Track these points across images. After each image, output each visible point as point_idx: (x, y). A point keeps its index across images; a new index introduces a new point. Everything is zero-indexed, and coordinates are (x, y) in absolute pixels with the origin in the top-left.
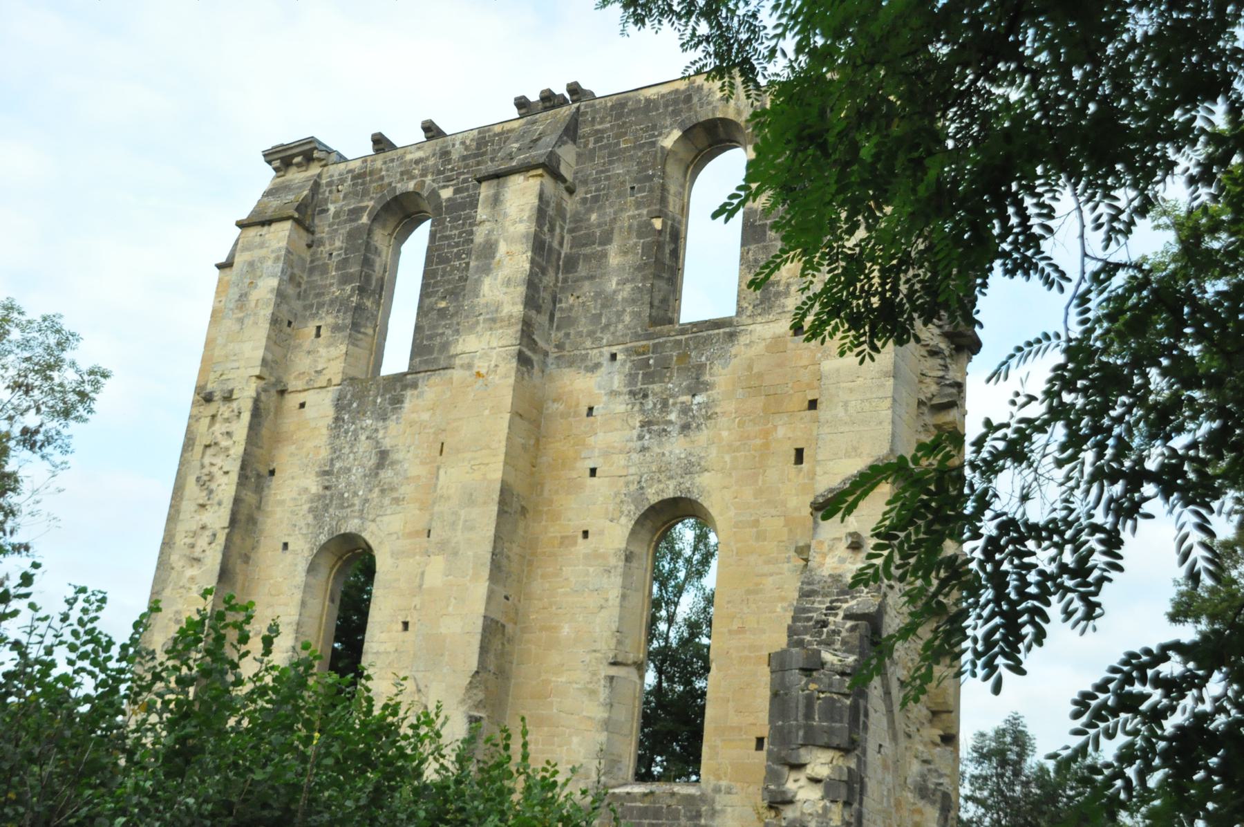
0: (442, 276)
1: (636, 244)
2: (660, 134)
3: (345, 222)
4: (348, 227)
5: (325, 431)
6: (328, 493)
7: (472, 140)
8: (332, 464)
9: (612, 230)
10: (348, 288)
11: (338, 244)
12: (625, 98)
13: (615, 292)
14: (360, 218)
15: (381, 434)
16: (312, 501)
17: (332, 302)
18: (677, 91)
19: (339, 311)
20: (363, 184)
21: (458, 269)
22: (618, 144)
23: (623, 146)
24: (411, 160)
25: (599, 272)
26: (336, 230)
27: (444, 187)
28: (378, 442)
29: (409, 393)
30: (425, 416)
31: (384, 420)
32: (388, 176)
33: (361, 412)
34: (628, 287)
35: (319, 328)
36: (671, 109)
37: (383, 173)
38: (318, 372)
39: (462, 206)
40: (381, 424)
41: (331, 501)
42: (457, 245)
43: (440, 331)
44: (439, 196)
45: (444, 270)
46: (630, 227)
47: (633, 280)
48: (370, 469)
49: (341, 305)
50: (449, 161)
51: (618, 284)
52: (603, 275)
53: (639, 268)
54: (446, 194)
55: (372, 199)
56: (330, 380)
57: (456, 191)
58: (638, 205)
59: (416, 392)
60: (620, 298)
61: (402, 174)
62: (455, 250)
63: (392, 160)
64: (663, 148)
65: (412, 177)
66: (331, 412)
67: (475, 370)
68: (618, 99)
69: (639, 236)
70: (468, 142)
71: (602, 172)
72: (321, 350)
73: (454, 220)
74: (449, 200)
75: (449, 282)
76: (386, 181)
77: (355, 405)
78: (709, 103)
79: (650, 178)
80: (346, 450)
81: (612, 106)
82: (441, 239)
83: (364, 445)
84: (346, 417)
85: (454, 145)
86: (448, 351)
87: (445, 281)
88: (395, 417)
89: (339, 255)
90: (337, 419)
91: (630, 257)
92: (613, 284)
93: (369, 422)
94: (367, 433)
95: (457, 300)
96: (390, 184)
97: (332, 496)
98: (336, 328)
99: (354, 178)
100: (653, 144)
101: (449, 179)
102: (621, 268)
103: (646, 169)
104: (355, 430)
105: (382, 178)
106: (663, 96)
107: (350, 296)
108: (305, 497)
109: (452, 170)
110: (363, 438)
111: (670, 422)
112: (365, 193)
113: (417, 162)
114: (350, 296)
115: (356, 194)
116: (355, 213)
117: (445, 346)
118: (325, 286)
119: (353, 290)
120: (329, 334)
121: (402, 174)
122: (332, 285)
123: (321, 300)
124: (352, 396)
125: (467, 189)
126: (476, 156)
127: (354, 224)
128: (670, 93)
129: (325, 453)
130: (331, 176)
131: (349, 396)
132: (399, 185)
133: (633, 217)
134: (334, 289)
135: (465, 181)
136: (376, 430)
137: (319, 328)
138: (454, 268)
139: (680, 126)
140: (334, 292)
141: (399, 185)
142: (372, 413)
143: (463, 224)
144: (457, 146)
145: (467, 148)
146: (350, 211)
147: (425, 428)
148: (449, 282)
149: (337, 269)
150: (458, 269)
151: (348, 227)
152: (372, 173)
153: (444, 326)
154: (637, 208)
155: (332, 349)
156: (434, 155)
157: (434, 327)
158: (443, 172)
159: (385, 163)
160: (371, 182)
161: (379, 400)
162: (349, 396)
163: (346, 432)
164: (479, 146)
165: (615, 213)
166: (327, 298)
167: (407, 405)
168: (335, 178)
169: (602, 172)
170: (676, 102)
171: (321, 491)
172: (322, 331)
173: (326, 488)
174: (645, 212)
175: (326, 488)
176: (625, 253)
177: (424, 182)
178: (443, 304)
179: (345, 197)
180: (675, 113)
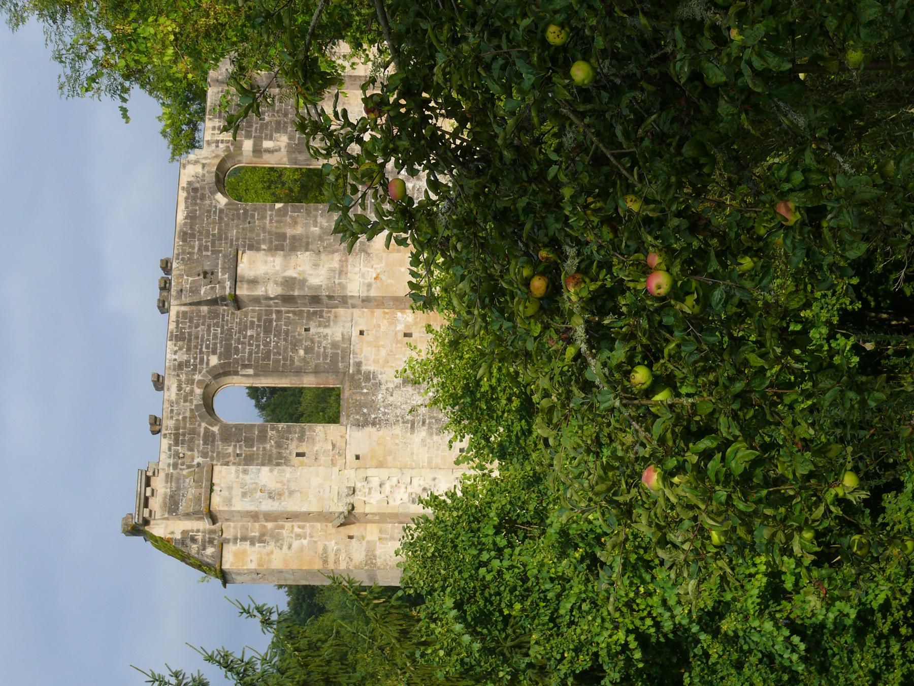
0: (280, 354)
1: (291, 217)
2: (215, 207)
3: (213, 446)
4: (218, 443)
5: (381, 433)
6: (427, 421)
7: (175, 345)
8: (407, 422)
9: (276, 233)
10: (270, 433)
11: (230, 450)
12: (180, 233)
13: (321, 228)
14: (213, 434)
15: (391, 385)
16: (431, 434)
17: (279, 445)
18: (187, 198)
19: (287, 439)
20: (184, 435)
21: (277, 343)
22: (214, 235)
23: (216, 232)
24: (177, 394)
25: (304, 240)
26: (218, 453)
27: (208, 364)
28: (396, 387)
29: (364, 368)
30: (383, 352)
31: (380, 384)
32: (184, 413)
33: (372, 406)
34: (319, 219)
35: (298, 455)
36: (198, 201)
37: (180, 417)
38: (334, 446)
39: (228, 348)
40: (383, 387)
41: (433, 417)
42: (258, 346)
43: (322, 350)
44: (215, 367)
45: (275, 354)
46: (277, 222)
47: (316, 217)
48: (415, 390)
49: (283, 438)
50: (188, 361)
51: (316, 226)
52: (308, 237)
53: (308, 213)
54: (214, 360)
55: (200, 425)
56: (342, 437)
57: (214, 353)
58: (263, 217)
59: (364, 362)
60: (326, 224)
61: (185, 401)
62: (262, 347)
63: (172, 411)
64: (226, 205)
65: (192, 391)
66: (370, 429)
67: (373, 280)
68: (179, 238)
69: (285, 214)
70: (176, 348)
71: (232, 244)
72: (316, 449)
73: (237, 350)
74: (220, 359)
75: (286, 349)
76: (188, 414)
77: (365, 411)
78: (204, 176)
79: (246, 211)
80: (398, 411)
81: (183, 241)
82: (249, 360)
83: (397, 398)
84: (373, 416)
85: (175, 360)
86: (338, 342)
87: (285, 352)
88: (379, 376)
89: (240, 447)
90: (374, 424)
91: (299, 220)
92: (316, 230)
93: (380, 396)
94: (388, 396)
95: (301, 340)
96: (192, 410)
97: (431, 418)
98: (301, 439)
99: (176, 444)
100: (221, 211)
101: (202, 360)
102: (307, 226)
103: (238, 214)
104: (385, 407)
105: (184, 418)
106: (187, 207)
107: (278, 431)
108: (428, 441)
109: (195, 358)
110: (391, 399)
111: (414, 187)
112: (193, 432)
113: (180, 388)
114: (278, 431)
115: (192, 440)
116: (209, 438)
117: (335, 345)
118: (264, 455)
119: (272, 429)
120: (304, 444)
121: (185, 401)
122: (264, 449)
123: (274, 456)
124: (358, 413)
125: (215, 344)
126: (190, 341)
127: (218, 437)
128: (186, 202)
129: (398, 430)
130: (169, 465)
131: (358, 417)
132: (195, 402)
133: (271, 220)
134: (268, 446)
135: (208, 347)
136: (387, 389)
137: (298, 455)
138: (276, 346)
139: (213, 193)
140: (271, 446)
141: (195, 402)
142: (374, 395)
143: (243, 343)
144: (176, 357)
145: (181, 349)
146: (205, 443)
147: (391, 351)
148: (286, 349)
149: (252, 446)
150: (277, 343)
151: (218, 443)
152: (177, 428)
153: (319, 347)
154: (266, 218)
155: (317, 438)
156: (178, 375)
157: (318, 354)
158: (195, 366)
159: (172, 417)
160: (184, 428)
161: (365, 391)
162: (358, 417)
163: (385, 414)
164: (183, 339)
165: (264, 232)
166: (274, 451)
167: (371, 368)
168: (171, 461)
169: (232, 244)
170: (194, 198)
171: (425, 428)
172: (300, 450)
173: (424, 423)
174: (269, 213)
175: (424, 423)
176: (296, 223)
177: (199, 381)
178: (302, 352)
179: (192, 450)
180: (203, 198)
